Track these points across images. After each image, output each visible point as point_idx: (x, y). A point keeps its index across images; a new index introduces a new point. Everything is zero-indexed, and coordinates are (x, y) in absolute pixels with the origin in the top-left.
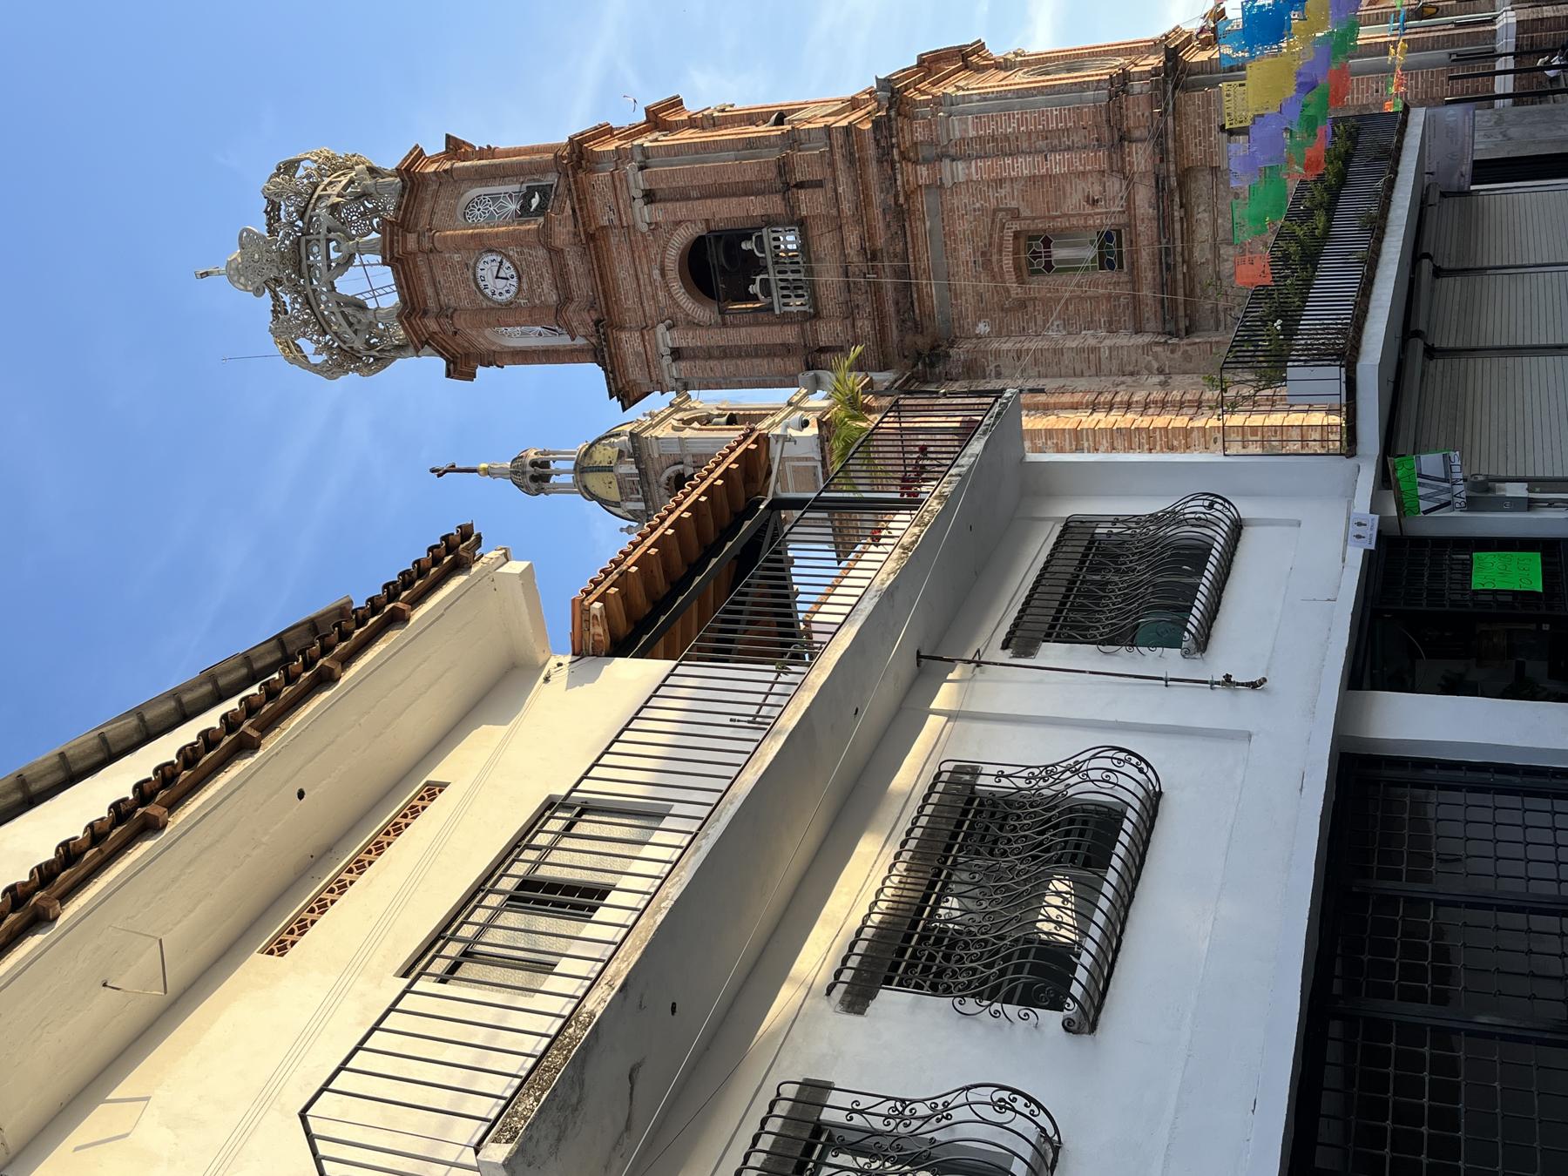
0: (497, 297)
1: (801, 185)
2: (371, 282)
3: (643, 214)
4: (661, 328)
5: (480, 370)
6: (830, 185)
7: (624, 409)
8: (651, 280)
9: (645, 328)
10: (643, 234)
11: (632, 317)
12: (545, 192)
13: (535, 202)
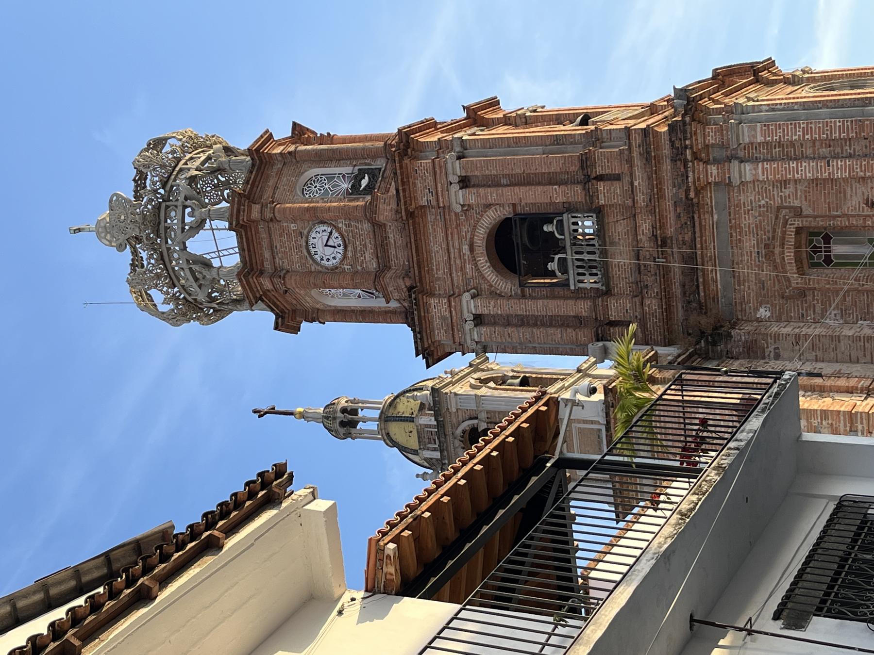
0: (324, 262)
1: (600, 178)
2: (217, 244)
3: (458, 197)
4: (466, 296)
5: (304, 325)
6: (626, 179)
7: (428, 366)
8: (460, 254)
9: (453, 296)
10: (456, 214)
11: (441, 285)
12: (373, 174)
13: (364, 182)
